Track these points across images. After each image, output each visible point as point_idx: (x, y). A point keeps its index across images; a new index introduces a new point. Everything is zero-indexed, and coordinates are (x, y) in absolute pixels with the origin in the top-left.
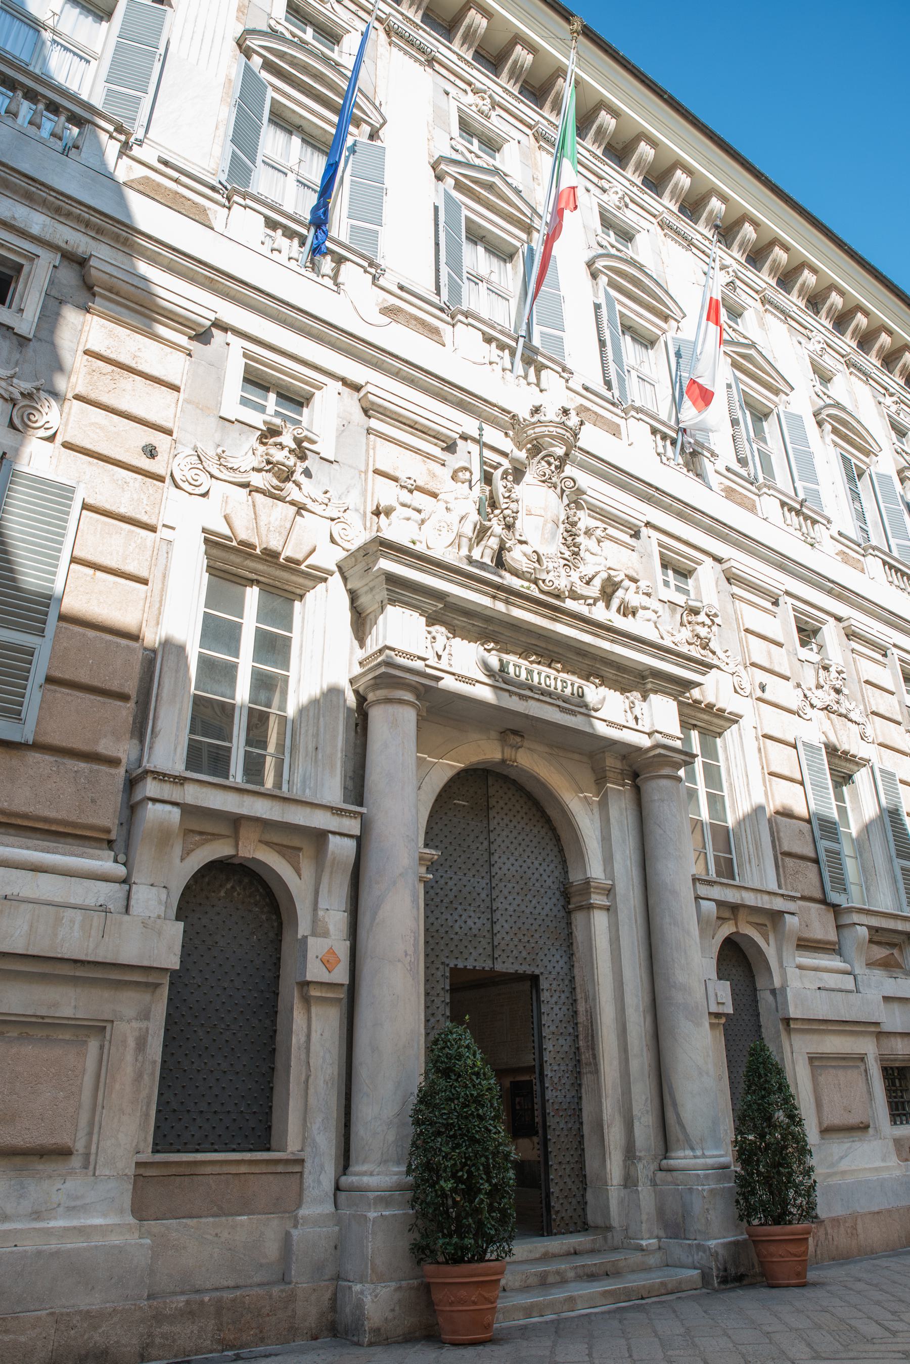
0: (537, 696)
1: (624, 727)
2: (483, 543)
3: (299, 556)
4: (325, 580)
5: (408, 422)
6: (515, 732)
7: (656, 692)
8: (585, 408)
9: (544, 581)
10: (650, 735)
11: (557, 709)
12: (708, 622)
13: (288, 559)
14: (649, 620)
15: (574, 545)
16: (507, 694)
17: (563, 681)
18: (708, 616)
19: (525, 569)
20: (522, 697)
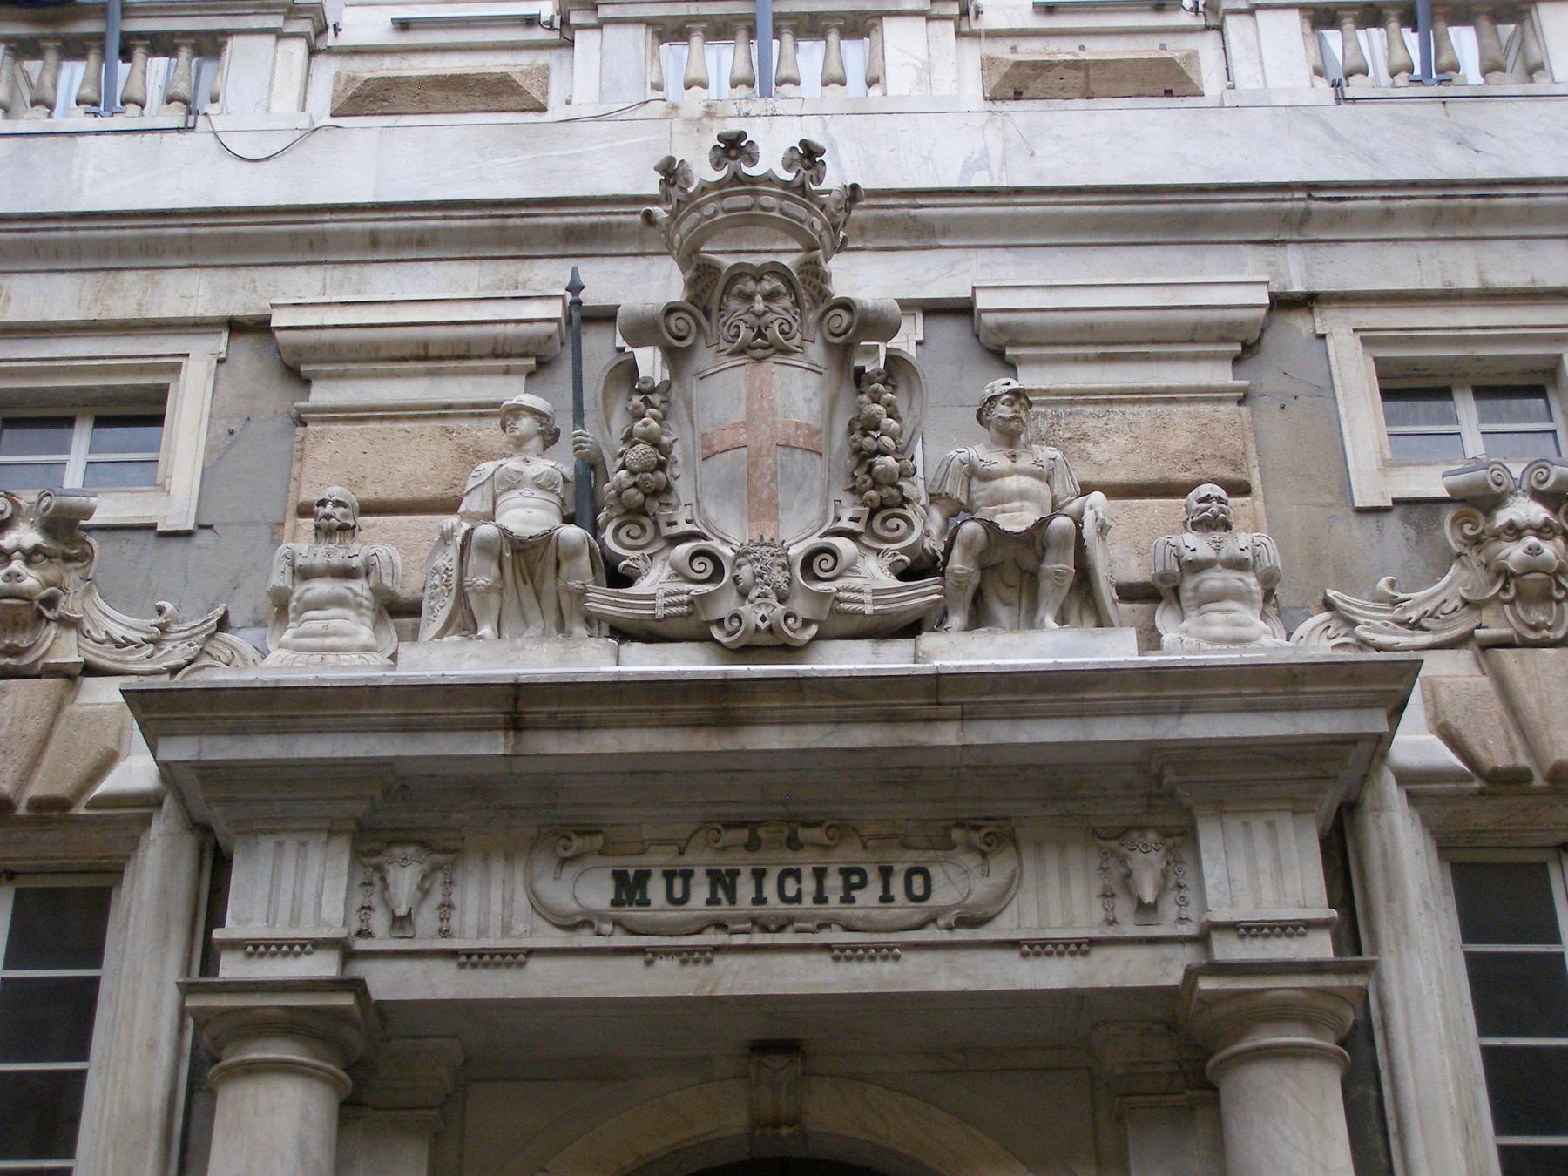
0: (739, 940)
1: (1093, 942)
2: (549, 585)
3: (61, 789)
4: (146, 822)
5: (406, 352)
6: (762, 1048)
7: (1220, 809)
8: (1035, 65)
9: (720, 623)
10: (1201, 940)
11: (825, 958)
12: (1536, 512)
13: (37, 804)
14: (1218, 597)
15: (876, 485)
16: (637, 962)
17: (846, 873)
18: (1538, 496)
19: (660, 613)
20: (687, 955)
